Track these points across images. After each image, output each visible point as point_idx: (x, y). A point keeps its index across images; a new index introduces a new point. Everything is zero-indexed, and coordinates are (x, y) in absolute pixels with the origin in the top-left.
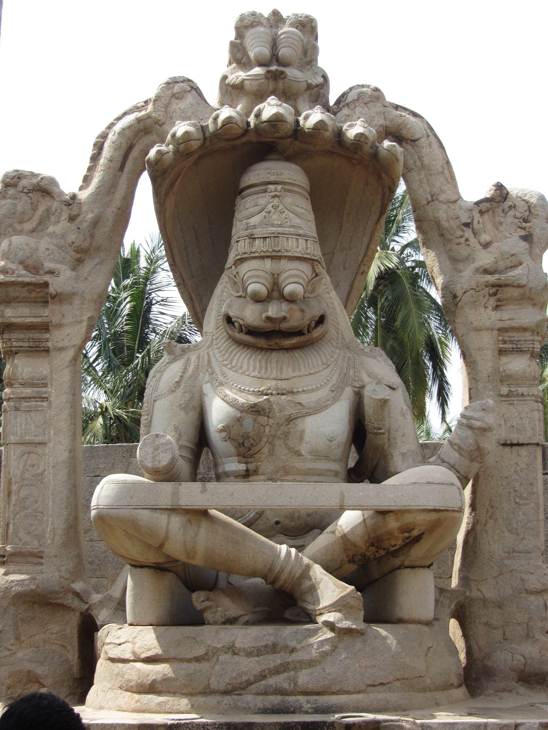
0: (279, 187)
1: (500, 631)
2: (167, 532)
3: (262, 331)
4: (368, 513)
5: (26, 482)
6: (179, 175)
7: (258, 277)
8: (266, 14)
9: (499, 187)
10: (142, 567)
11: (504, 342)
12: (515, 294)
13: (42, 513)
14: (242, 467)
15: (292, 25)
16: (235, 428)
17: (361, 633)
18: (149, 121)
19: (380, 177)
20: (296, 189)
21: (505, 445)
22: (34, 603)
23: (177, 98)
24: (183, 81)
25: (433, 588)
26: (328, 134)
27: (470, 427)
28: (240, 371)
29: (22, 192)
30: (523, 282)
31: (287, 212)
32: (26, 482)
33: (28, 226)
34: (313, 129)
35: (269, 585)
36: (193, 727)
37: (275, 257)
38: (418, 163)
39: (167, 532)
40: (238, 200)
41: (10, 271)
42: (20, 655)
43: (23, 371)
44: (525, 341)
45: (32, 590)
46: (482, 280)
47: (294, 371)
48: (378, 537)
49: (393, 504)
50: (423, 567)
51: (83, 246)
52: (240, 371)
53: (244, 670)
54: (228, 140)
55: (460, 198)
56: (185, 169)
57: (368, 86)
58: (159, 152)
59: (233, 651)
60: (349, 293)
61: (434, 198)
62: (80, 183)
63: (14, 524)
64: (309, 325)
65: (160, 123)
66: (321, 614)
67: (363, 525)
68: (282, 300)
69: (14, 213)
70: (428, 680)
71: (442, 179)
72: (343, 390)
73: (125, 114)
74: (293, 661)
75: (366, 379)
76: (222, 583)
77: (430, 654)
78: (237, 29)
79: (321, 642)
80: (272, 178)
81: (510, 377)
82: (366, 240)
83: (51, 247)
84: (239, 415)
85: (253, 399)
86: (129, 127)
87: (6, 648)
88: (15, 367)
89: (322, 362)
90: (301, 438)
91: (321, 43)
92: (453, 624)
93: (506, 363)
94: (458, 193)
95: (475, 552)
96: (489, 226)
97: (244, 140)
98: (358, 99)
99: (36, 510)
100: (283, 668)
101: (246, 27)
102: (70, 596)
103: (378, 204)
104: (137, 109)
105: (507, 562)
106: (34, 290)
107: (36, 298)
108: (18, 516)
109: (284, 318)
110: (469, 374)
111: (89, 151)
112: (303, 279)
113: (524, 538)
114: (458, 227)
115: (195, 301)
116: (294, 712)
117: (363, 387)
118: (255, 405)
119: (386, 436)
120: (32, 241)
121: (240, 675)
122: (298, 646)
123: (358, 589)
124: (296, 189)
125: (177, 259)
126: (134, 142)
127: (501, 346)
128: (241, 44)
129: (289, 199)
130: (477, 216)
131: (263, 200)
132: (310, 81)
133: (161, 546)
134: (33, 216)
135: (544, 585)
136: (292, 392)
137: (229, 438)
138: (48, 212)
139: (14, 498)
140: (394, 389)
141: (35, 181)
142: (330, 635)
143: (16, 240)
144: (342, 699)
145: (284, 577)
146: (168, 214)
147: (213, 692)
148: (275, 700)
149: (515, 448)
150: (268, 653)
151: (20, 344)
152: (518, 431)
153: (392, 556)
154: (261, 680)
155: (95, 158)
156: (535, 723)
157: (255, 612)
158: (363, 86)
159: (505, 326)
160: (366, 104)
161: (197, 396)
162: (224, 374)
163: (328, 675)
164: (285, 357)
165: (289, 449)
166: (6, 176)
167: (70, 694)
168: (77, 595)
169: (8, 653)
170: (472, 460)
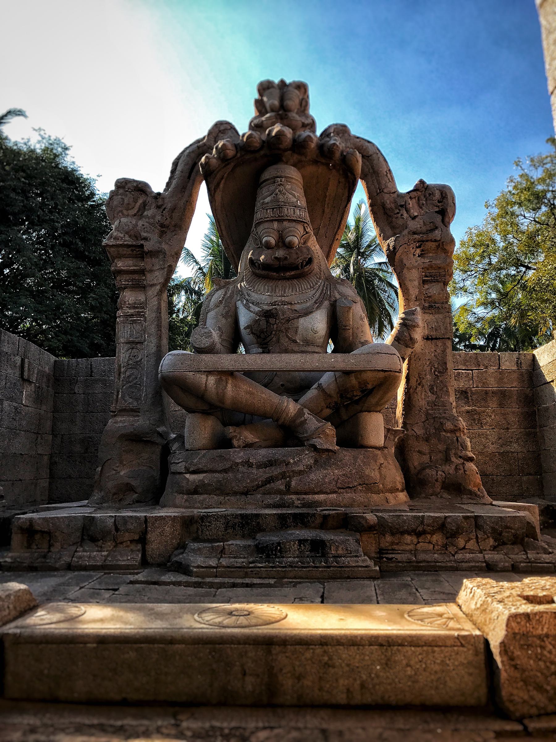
0: (283, 179)
1: (428, 456)
4: (338, 374)
7: (269, 232)
8: (277, 81)
9: (422, 182)
11: (426, 276)
13: (139, 384)
14: (260, 350)
17: (334, 452)
18: (205, 147)
23: (222, 133)
25: (383, 428)
26: (313, 145)
28: (259, 293)
29: (127, 191)
36: (218, 517)
37: (280, 220)
40: (258, 191)
41: (120, 239)
42: (122, 473)
43: (129, 299)
50: (376, 412)
52: (259, 293)
55: (397, 191)
58: (207, 157)
61: (382, 191)
62: (164, 186)
63: (122, 392)
64: (302, 263)
66: (308, 440)
70: (381, 486)
73: (191, 145)
75: (338, 296)
78: (259, 91)
81: (430, 297)
82: (339, 219)
83: (145, 224)
84: (258, 318)
85: (266, 307)
86: (193, 152)
89: (310, 286)
93: (427, 289)
94: (396, 188)
96: (416, 206)
97: (262, 153)
99: (135, 384)
102: (156, 435)
104: (198, 141)
106: (135, 250)
107: (136, 255)
108: (124, 387)
111: (169, 168)
115: (236, 259)
116: (288, 507)
117: (336, 301)
118: (267, 311)
119: (351, 331)
121: (252, 481)
123: (332, 424)
125: (224, 233)
126: (197, 161)
132: (303, 121)
135: (456, 426)
136: (291, 304)
137: (252, 333)
138: (144, 205)
141: (135, 184)
143: (124, 220)
144: (322, 497)
146: (217, 204)
148: (277, 498)
150: (271, 465)
151: (127, 283)
154: (266, 485)
155: (173, 172)
161: (233, 309)
164: (287, 283)
165: (289, 338)
168: (160, 435)
169: (114, 472)
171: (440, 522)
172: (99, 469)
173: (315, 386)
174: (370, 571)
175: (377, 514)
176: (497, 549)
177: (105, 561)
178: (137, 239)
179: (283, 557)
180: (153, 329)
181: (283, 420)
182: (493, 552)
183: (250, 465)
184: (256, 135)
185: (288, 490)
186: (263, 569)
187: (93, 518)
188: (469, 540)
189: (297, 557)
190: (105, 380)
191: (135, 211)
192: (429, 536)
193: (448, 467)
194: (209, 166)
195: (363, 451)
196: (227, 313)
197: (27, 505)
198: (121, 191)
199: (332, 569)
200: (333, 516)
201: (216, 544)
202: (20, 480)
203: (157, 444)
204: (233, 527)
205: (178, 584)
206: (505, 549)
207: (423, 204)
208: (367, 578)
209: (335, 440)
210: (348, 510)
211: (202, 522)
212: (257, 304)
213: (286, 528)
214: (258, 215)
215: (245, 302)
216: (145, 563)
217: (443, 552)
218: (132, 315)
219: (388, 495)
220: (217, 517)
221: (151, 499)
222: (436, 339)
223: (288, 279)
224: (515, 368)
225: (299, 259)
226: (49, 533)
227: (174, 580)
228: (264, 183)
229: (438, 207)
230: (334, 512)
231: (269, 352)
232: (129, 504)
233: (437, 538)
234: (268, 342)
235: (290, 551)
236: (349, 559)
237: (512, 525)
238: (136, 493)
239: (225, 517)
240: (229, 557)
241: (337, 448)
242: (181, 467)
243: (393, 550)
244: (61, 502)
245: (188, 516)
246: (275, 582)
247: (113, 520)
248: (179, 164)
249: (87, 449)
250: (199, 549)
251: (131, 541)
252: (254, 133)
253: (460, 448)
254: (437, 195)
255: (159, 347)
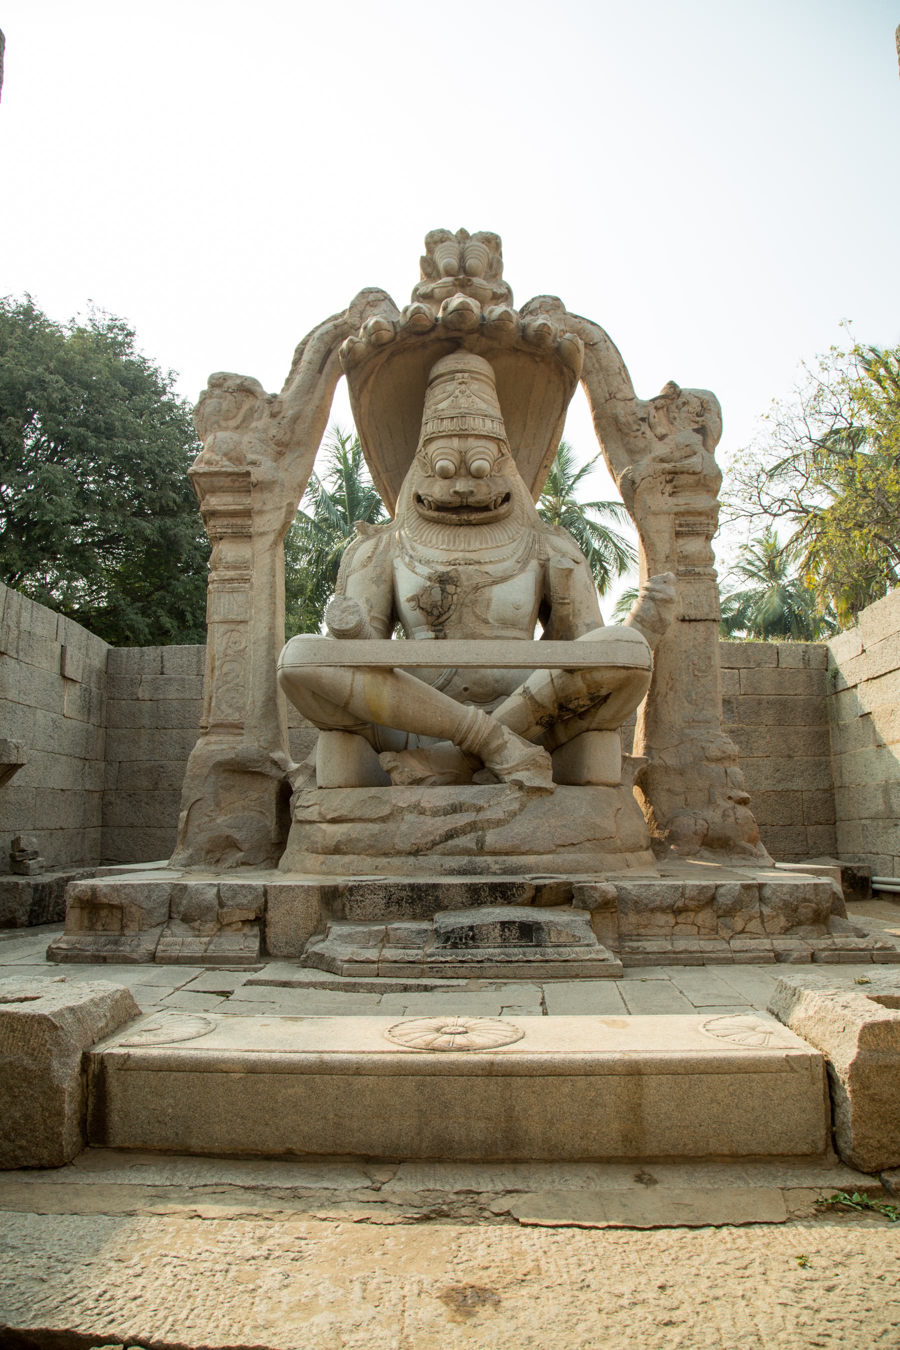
0: (466, 375)
2: (351, 690)
3: (450, 506)
4: (556, 672)
5: (228, 658)
6: (373, 372)
7: (446, 454)
8: (454, 232)
9: (672, 385)
10: (330, 730)
11: (681, 525)
12: (690, 481)
13: (243, 686)
14: (432, 634)
15: (478, 240)
16: (424, 597)
17: (551, 792)
19: (562, 373)
20: (482, 377)
21: (683, 620)
22: (234, 771)
24: (377, 292)
26: (512, 326)
27: (652, 599)
30: (698, 470)
31: (473, 397)
32: (228, 658)
33: (233, 423)
34: (498, 320)
35: (458, 747)
38: (597, 366)
39: (351, 690)
40: (428, 391)
42: (219, 821)
44: (701, 524)
45: (232, 759)
46: (659, 467)
47: (481, 544)
48: (566, 696)
49: (582, 661)
50: (610, 730)
51: (283, 440)
53: (430, 829)
54: (419, 334)
56: (377, 368)
57: (549, 297)
58: (351, 340)
59: (419, 810)
60: (533, 485)
61: (612, 396)
62: (283, 385)
65: (356, 327)
66: (510, 773)
67: (550, 685)
68: (470, 477)
69: (219, 411)
70: (619, 841)
71: (619, 379)
72: (528, 562)
73: (323, 323)
74: (480, 821)
75: (551, 553)
76: (411, 746)
77: (619, 816)
78: (428, 244)
79: (511, 800)
80: (459, 367)
81: (686, 557)
82: (549, 435)
83: (254, 440)
84: (428, 583)
85: (442, 569)
86: (327, 333)
87: (206, 814)
88: (221, 551)
90: (488, 606)
91: (505, 260)
92: (637, 791)
95: (656, 722)
96: (664, 421)
97: (433, 335)
98: (540, 307)
99: (237, 685)
100: (473, 827)
101: (436, 243)
103: (561, 401)
104: (335, 318)
105: (687, 731)
108: (220, 690)
109: (472, 492)
110: (647, 555)
111: (291, 356)
112: (489, 456)
113: (703, 709)
114: (635, 422)
115: (390, 493)
116: (481, 873)
117: (548, 560)
118: (443, 573)
119: (571, 606)
120: (236, 436)
121: (424, 835)
122: (486, 806)
123: (546, 749)
124: (482, 377)
125: (373, 454)
127: (678, 529)
128: (432, 259)
129: (475, 386)
130: (653, 412)
131: (450, 387)
132: (495, 290)
133: (347, 704)
134: (238, 413)
135: (724, 752)
136: (480, 563)
138: (252, 410)
139: (217, 673)
140: (578, 563)
141: (238, 382)
142: (518, 794)
143: (221, 435)
144: (531, 860)
145: (471, 736)
146: (362, 411)
147: (399, 853)
148: (464, 860)
149: (692, 623)
151: (225, 530)
152: (696, 607)
153: (580, 719)
154: (446, 840)
155: (296, 363)
156: (736, 885)
157: (443, 774)
158: (544, 297)
159: (682, 510)
160: (547, 312)
161: (388, 570)
162: (413, 549)
163: (518, 834)
165: (477, 616)
166: (212, 377)
167: (267, 859)
168: (275, 763)
169: (207, 819)
170: (654, 631)
171: (709, 894)
172: (184, 814)
173: (520, 690)
174: (610, 966)
175: (616, 883)
176: (791, 931)
177: (206, 951)
178: (241, 464)
179: (478, 947)
180: (263, 602)
181: (469, 743)
182: (784, 936)
183: (422, 812)
184: (426, 309)
185: (481, 850)
186: (447, 965)
187: (185, 887)
188: (751, 919)
189: (499, 947)
190: (183, 680)
191: (238, 420)
192: (692, 914)
193: (711, 813)
194: (354, 354)
195: (589, 790)
196: (379, 577)
197: (72, 867)
198: (217, 392)
199: (552, 964)
200: (550, 887)
201: (376, 928)
202: (61, 828)
203: (271, 778)
204: (399, 902)
205: (323, 985)
206: (802, 930)
207: (675, 419)
208: (604, 977)
209: (551, 773)
210: (573, 878)
211: (351, 895)
212: (428, 562)
213: (480, 905)
214: (428, 428)
215: (407, 559)
216: (265, 954)
217: (712, 937)
218: (231, 580)
219: (628, 856)
220: (373, 889)
221: (264, 861)
222: (695, 620)
223: (474, 525)
224: (801, 666)
225: (491, 495)
226: (121, 908)
227: (314, 980)
228: (437, 381)
229: (697, 422)
230: (552, 881)
231: (445, 637)
232: (231, 867)
233: (705, 917)
234: (444, 622)
235: (488, 938)
236: (577, 949)
237: (812, 897)
238: (241, 851)
239: (386, 887)
240: (395, 947)
241: (551, 785)
242: (311, 814)
243: (638, 935)
244: (137, 862)
245: (329, 887)
246: (467, 984)
247: (215, 890)
248: (306, 351)
249: (156, 783)
250: (350, 935)
251: (245, 922)
252: (421, 305)
253: (730, 785)
254: (695, 406)
255: (272, 628)
